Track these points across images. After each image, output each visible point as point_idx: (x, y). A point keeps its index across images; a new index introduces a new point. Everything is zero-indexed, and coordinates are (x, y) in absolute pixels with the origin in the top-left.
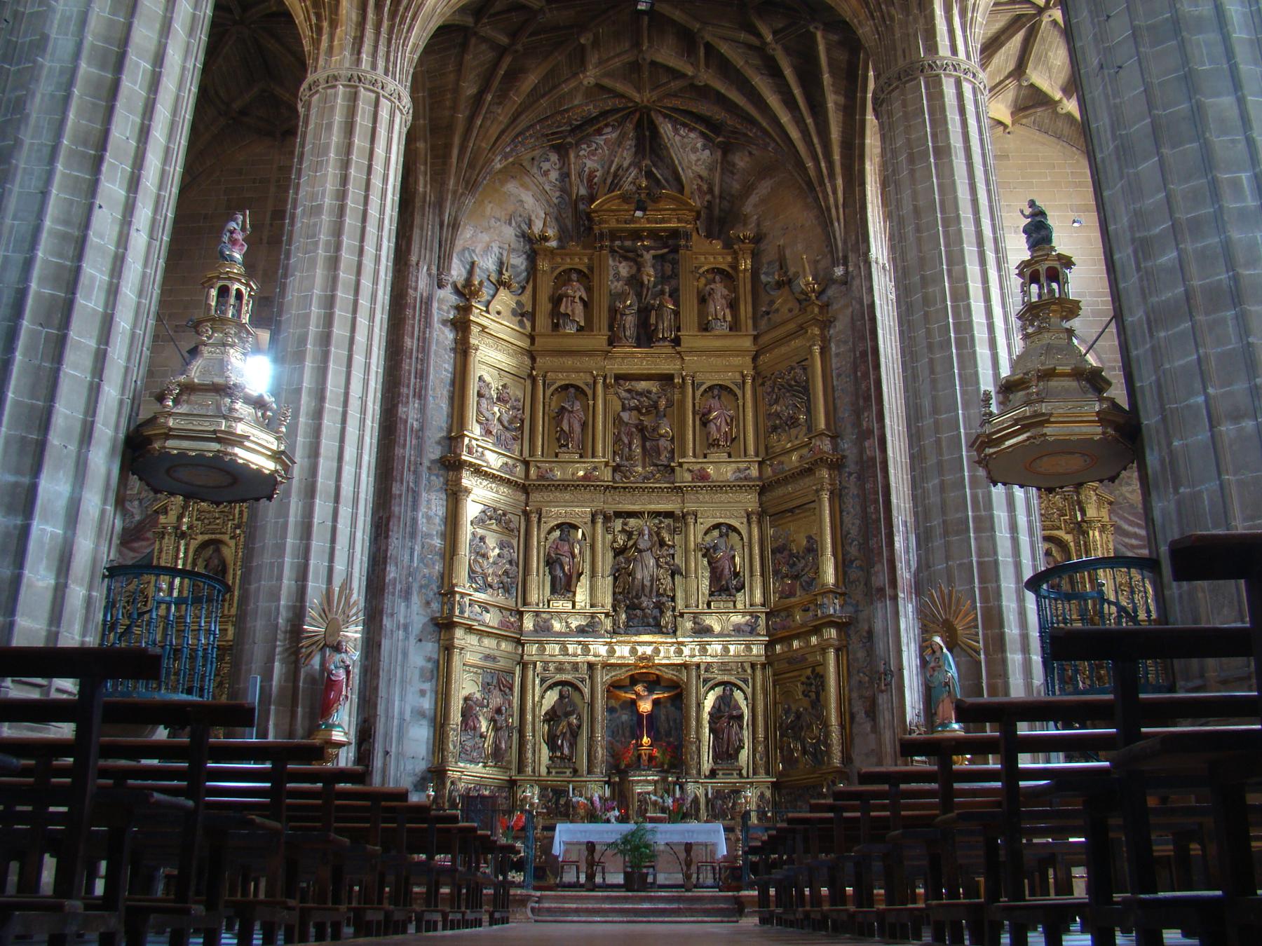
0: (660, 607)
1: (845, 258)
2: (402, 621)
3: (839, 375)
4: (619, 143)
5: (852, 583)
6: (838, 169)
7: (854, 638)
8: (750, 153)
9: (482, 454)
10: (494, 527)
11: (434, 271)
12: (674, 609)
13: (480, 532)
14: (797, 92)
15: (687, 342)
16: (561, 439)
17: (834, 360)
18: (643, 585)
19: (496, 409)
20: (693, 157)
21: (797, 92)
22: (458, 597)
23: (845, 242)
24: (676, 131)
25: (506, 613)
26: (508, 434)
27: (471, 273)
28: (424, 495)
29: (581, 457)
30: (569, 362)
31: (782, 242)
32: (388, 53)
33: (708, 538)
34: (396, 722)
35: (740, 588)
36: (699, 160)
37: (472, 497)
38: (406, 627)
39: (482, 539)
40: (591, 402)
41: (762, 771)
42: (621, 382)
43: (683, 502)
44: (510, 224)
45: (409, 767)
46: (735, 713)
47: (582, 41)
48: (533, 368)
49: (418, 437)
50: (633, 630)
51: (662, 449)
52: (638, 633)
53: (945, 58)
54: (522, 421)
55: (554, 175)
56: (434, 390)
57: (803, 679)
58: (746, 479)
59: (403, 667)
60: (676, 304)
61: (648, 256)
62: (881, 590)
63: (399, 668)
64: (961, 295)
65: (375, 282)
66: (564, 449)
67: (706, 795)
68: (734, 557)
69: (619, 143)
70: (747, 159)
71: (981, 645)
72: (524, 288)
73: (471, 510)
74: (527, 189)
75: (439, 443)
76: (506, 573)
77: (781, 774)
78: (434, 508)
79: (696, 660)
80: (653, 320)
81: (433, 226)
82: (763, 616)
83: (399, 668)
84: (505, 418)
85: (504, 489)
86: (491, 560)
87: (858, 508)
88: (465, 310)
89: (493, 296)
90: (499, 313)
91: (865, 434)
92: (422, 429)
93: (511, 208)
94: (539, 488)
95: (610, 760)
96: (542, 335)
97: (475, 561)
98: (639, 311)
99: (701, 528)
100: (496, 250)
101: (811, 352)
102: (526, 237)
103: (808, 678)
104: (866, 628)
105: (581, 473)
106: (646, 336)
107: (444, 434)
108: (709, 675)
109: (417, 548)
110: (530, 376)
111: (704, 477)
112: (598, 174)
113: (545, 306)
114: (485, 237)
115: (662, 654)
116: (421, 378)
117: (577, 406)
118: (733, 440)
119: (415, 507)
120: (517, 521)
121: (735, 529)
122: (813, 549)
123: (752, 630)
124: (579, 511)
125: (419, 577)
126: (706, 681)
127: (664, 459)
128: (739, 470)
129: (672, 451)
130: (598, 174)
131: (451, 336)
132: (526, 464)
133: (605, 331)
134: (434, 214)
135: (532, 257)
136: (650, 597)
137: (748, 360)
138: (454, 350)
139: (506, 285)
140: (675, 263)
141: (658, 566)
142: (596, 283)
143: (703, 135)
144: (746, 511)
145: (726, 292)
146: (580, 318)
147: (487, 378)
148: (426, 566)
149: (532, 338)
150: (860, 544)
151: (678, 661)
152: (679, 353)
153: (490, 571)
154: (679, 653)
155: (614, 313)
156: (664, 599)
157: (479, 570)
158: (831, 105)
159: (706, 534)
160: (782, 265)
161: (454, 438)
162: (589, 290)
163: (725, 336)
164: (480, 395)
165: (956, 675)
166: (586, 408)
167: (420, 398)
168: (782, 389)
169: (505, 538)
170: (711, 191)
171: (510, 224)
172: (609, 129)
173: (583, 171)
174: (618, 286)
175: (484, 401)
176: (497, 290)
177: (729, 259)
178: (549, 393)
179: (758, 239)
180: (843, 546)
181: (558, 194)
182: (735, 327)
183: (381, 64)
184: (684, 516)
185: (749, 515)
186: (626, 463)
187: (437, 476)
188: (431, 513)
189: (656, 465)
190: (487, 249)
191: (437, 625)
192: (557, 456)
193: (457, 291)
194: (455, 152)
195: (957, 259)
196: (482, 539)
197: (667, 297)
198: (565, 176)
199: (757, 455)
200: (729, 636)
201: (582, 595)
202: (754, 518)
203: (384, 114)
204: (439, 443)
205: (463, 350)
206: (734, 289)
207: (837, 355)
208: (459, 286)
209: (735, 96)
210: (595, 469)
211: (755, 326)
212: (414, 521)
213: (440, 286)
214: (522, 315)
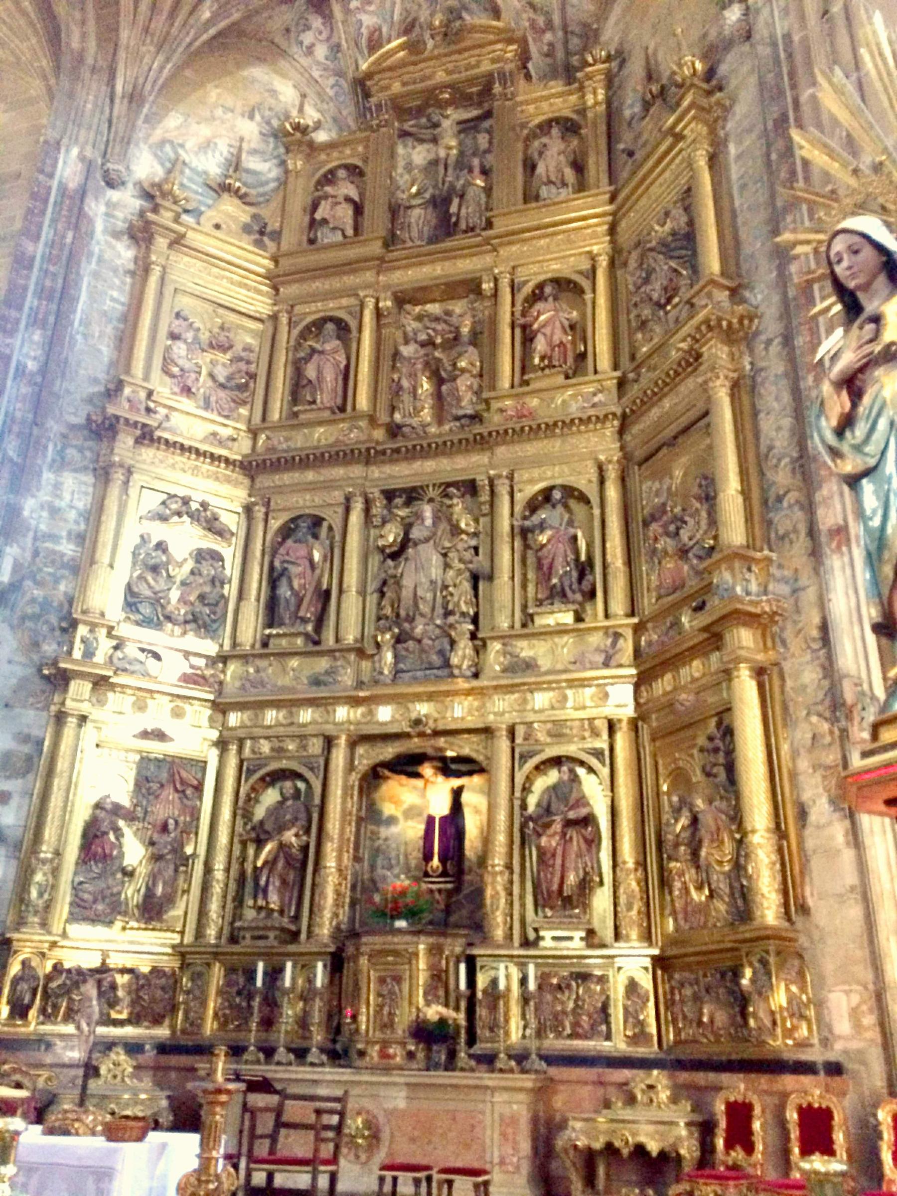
3: (743, 187)
5: (782, 538)
7: (795, 644)
26: (222, 394)
41: (634, 934)
42: (408, 307)
46: (572, 815)
55: (321, 51)
57: (701, 741)
67: (523, 981)
68: (575, 538)
74: (284, 75)
77: (671, 941)
78: (67, 496)
82: (629, 633)
93: (254, 99)
97: (141, 578)
103: (711, 739)
104: (817, 620)
114: (205, 131)
126: (524, 758)
141: (447, 566)
148: (39, 584)
150: (793, 461)
157: (148, 593)
167: (43, 327)
170: (549, 26)
171: (251, 117)
173: (360, 34)
181: (332, 81)
187: (81, 450)
188: (63, 504)
189: (457, 418)
190: (207, 145)
199: (616, 367)
207: (739, 157)
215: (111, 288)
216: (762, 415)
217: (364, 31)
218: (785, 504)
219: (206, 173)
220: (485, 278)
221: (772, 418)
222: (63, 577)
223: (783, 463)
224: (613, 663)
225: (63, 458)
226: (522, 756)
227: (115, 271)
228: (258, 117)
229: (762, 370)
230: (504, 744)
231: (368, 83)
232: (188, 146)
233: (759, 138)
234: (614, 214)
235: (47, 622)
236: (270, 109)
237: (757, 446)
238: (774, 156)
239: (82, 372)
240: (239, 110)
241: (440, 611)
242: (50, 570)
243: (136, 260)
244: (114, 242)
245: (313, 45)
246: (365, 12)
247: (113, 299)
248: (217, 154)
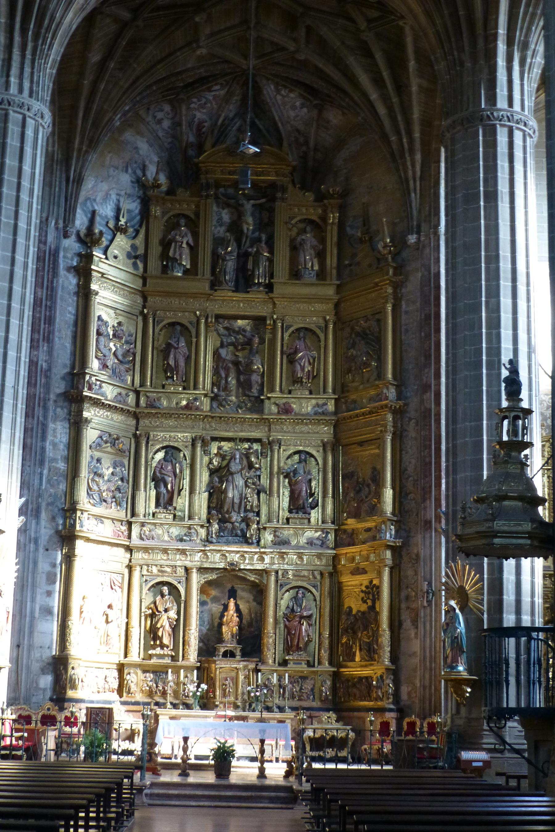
0: (247, 521)
1: (419, 226)
2: (33, 535)
4: (227, 99)
6: (418, 145)
9: (101, 387)
10: (109, 449)
11: (61, 225)
12: (258, 523)
13: (97, 454)
14: (385, 74)
15: (278, 290)
16: (168, 371)
17: (404, 317)
18: (233, 503)
19: (112, 345)
20: (292, 114)
21: (385, 74)
22: (79, 513)
23: (419, 212)
25: (118, 524)
26: (122, 368)
27: (92, 221)
28: (51, 426)
29: (184, 388)
30: (175, 302)
31: (364, 200)
32: (32, 74)
33: (289, 461)
34: (28, 619)
35: (314, 506)
36: (297, 116)
37: (91, 425)
38: (36, 541)
39: (99, 461)
40: (194, 340)
42: (221, 320)
43: (269, 430)
44: (127, 171)
45: (38, 655)
47: (197, 19)
48: (144, 307)
49: (47, 377)
50: (224, 539)
51: (253, 383)
52: (228, 543)
53: (500, 110)
54: (134, 355)
55: (166, 124)
56: (60, 331)
58: (323, 413)
59: (33, 573)
60: (271, 252)
61: (248, 206)
62: (428, 523)
63: (30, 575)
64: (495, 324)
65: (24, 286)
66: (170, 381)
69: (227, 99)
71: (485, 608)
72: (137, 232)
73: (90, 435)
75: (63, 378)
76: (118, 489)
79: (275, 567)
80: (250, 266)
81: (60, 182)
83: (30, 575)
84: (120, 353)
85: (118, 417)
86: (106, 478)
88: (88, 258)
89: (111, 241)
90: (116, 257)
91: (426, 388)
92: (49, 369)
94: (149, 415)
95: (201, 644)
96: (152, 277)
97: (93, 480)
98: (239, 256)
99: (284, 454)
100: (114, 197)
101: (384, 308)
102: (140, 183)
105: (184, 403)
106: (244, 282)
107: (68, 370)
108: (284, 580)
109: (45, 472)
110: (142, 313)
111: (286, 410)
112: (206, 124)
113: (156, 250)
114: (104, 186)
115: (247, 561)
116: (50, 324)
117: (182, 344)
118: (314, 377)
119: (44, 438)
120: (126, 443)
121: (312, 456)
122: (377, 480)
123: (323, 544)
124: (181, 437)
125: (46, 496)
127: (255, 391)
128: (317, 405)
129: (262, 385)
130: (206, 124)
131: (74, 281)
132: (137, 393)
133: (208, 274)
134: (61, 172)
135: (145, 203)
136: (239, 513)
137: (331, 306)
138: (77, 294)
139: (123, 231)
140: (271, 211)
141: (247, 486)
142: (201, 230)
143: (301, 96)
144: (322, 441)
145: (315, 243)
146: (186, 262)
147: (105, 317)
148: (52, 486)
149: (144, 279)
151: (259, 567)
152: (271, 298)
153: (105, 488)
154: (262, 559)
155: (216, 258)
156: (250, 515)
158: (414, 88)
159: (288, 458)
160: (366, 222)
161: (77, 374)
162: (195, 235)
163: (312, 285)
164: (99, 334)
165: (464, 631)
166: (189, 344)
167: (48, 342)
168: (358, 339)
169: (118, 459)
170: (306, 143)
171: (127, 171)
172: (217, 87)
173: (193, 121)
174: (221, 231)
175: (102, 339)
176: (114, 236)
177: (320, 211)
178: (157, 330)
179: (345, 194)
180: (401, 481)
181: (170, 140)
182: (321, 275)
183: (26, 85)
184: (270, 443)
185: (324, 445)
186: (222, 393)
187: (62, 408)
188: (57, 440)
189: (249, 396)
191: (61, 536)
192: (163, 387)
193: (79, 239)
194: (81, 114)
195: (494, 293)
196: (99, 461)
197: (263, 244)
198: (177, 124)
199: (334, 392)
200: (303, 547)
201: (182, 502)
202: (329, 448)
203: (29, 133)
204: (63, 378)
205: (85, 295)
206: (322, 240)
208: (82, 235)
209: (330, 70)
210: (196, 399)
211: (339, 276)
212: (43, 449)
213: (66, 236)
214: (136, 257)
215: (68, 306)
216: (404, 452)
217: (196, 120)
219: (106, 216)
220: (268, 318)
222: (61, 481)
224: (325, 546)
225: (55, 414)
226: (281, 585)
227: (69, 294)
228: (130, 170)
229: (406, 430)
230: (273, 578)
231: (200, 165)
232: (98, 200)
234: (339, 299)
235: (57, 506)
236: (136, 162)
237: (400, 466)
238: (423, 334)
239: (59, 361)
240: (120, 167)
241: (243, 509)
242: (55, 478)
243: (78, 285)
244: (68, 274)
245: (162, 119)
246: (200, 112)
247: (70, 313)
248: (111, 203)
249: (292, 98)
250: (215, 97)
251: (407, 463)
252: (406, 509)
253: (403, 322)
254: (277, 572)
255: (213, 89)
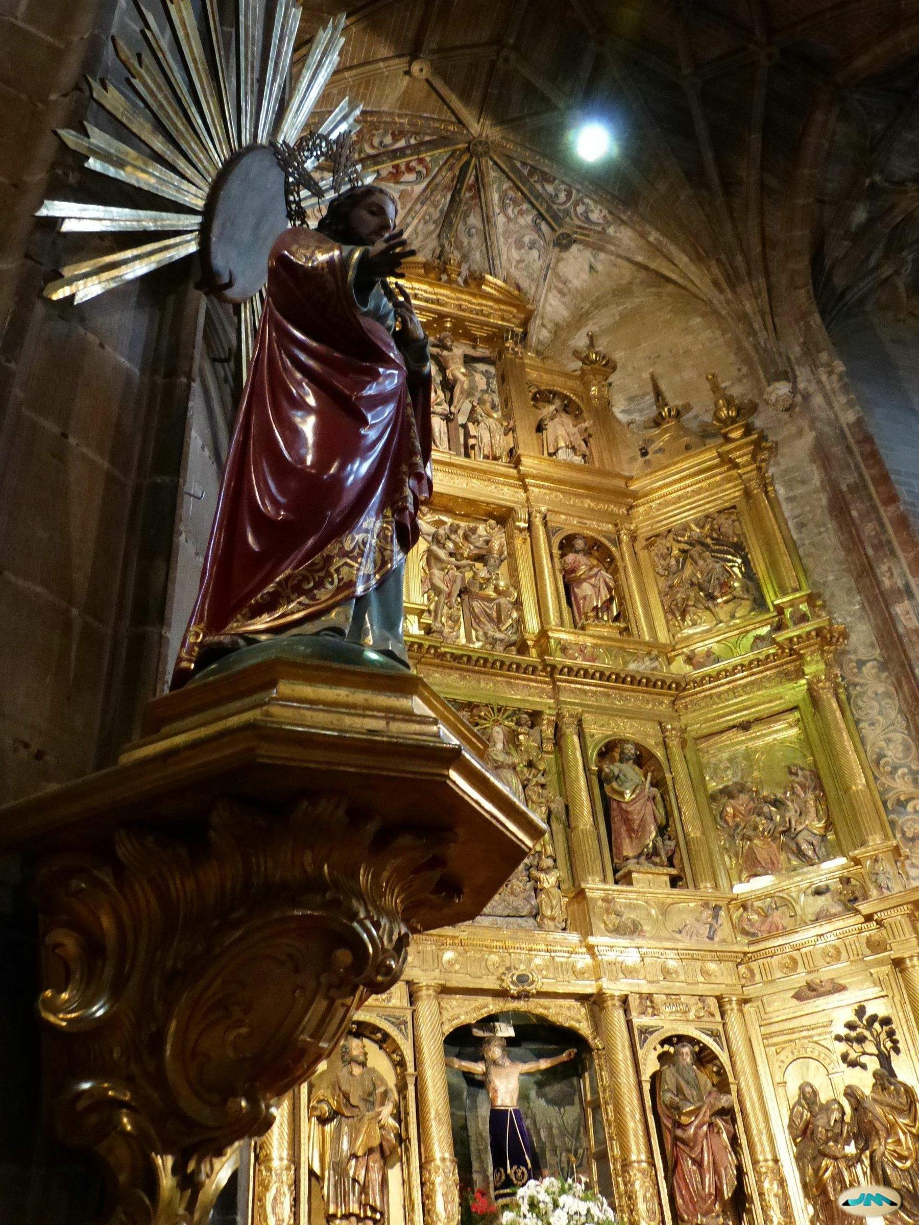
3: (801, 526)
8: (592, 268)
20: (515, 255)
24: (503, 207)
70: (585, 276)
87: (893, 714)
172: (411, 177)
207: (790, 499)
218: (910, 808)
221: (878, 730)
223: (900, 772)
229: (855, 685)
233: (817, 491)
249: (521, 227)
250: (403, 194)
251: (883, 744)
252: (909, 834)
253: (787, 515)
254: (625, 1000)
255: (402, 179)
